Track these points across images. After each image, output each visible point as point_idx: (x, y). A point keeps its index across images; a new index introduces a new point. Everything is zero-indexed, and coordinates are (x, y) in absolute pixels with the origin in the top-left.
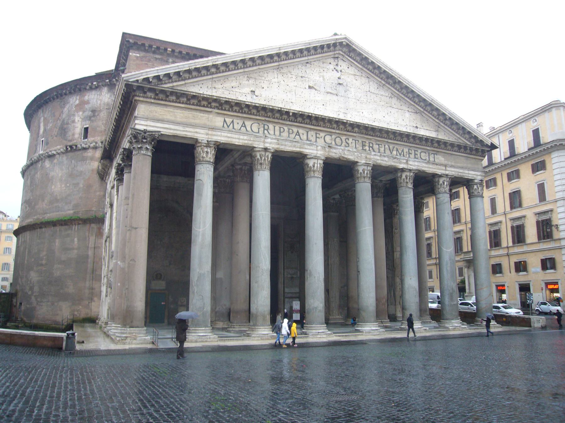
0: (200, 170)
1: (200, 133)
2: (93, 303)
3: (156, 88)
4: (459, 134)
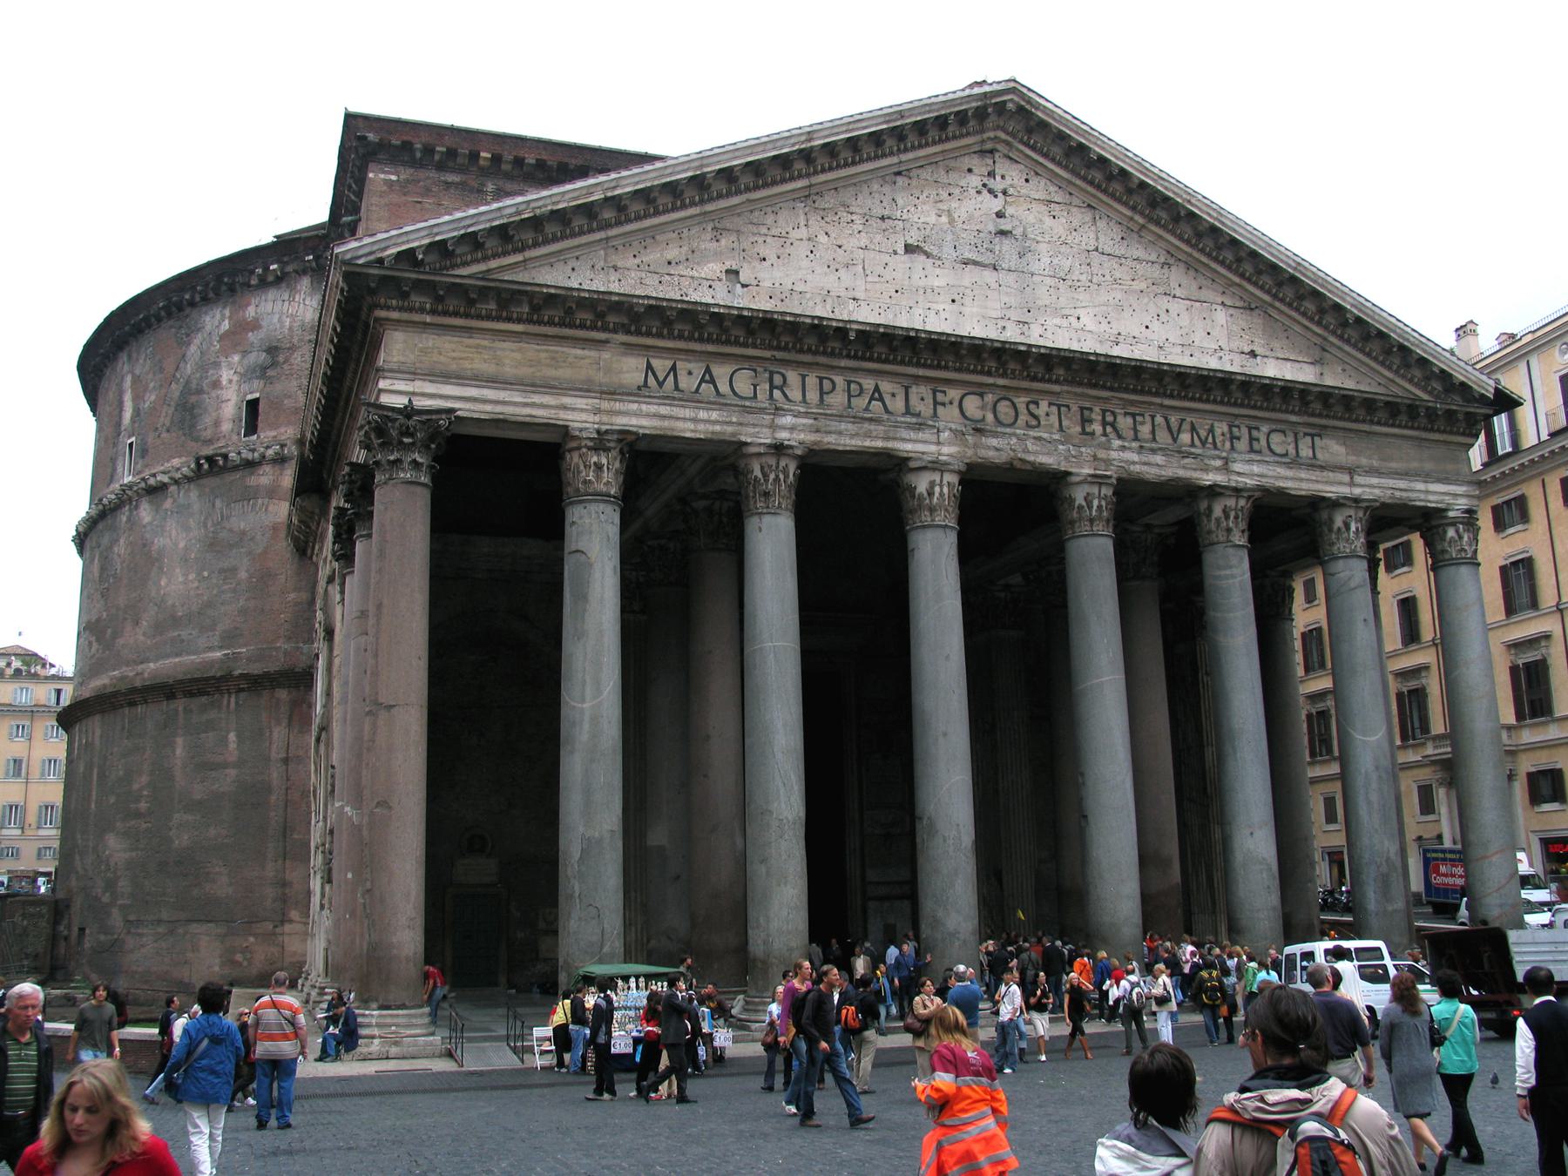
0: (579, 522)
1: (574, 409)
2: (287, 928)
3: (438, 278)
4: (1389, 368)
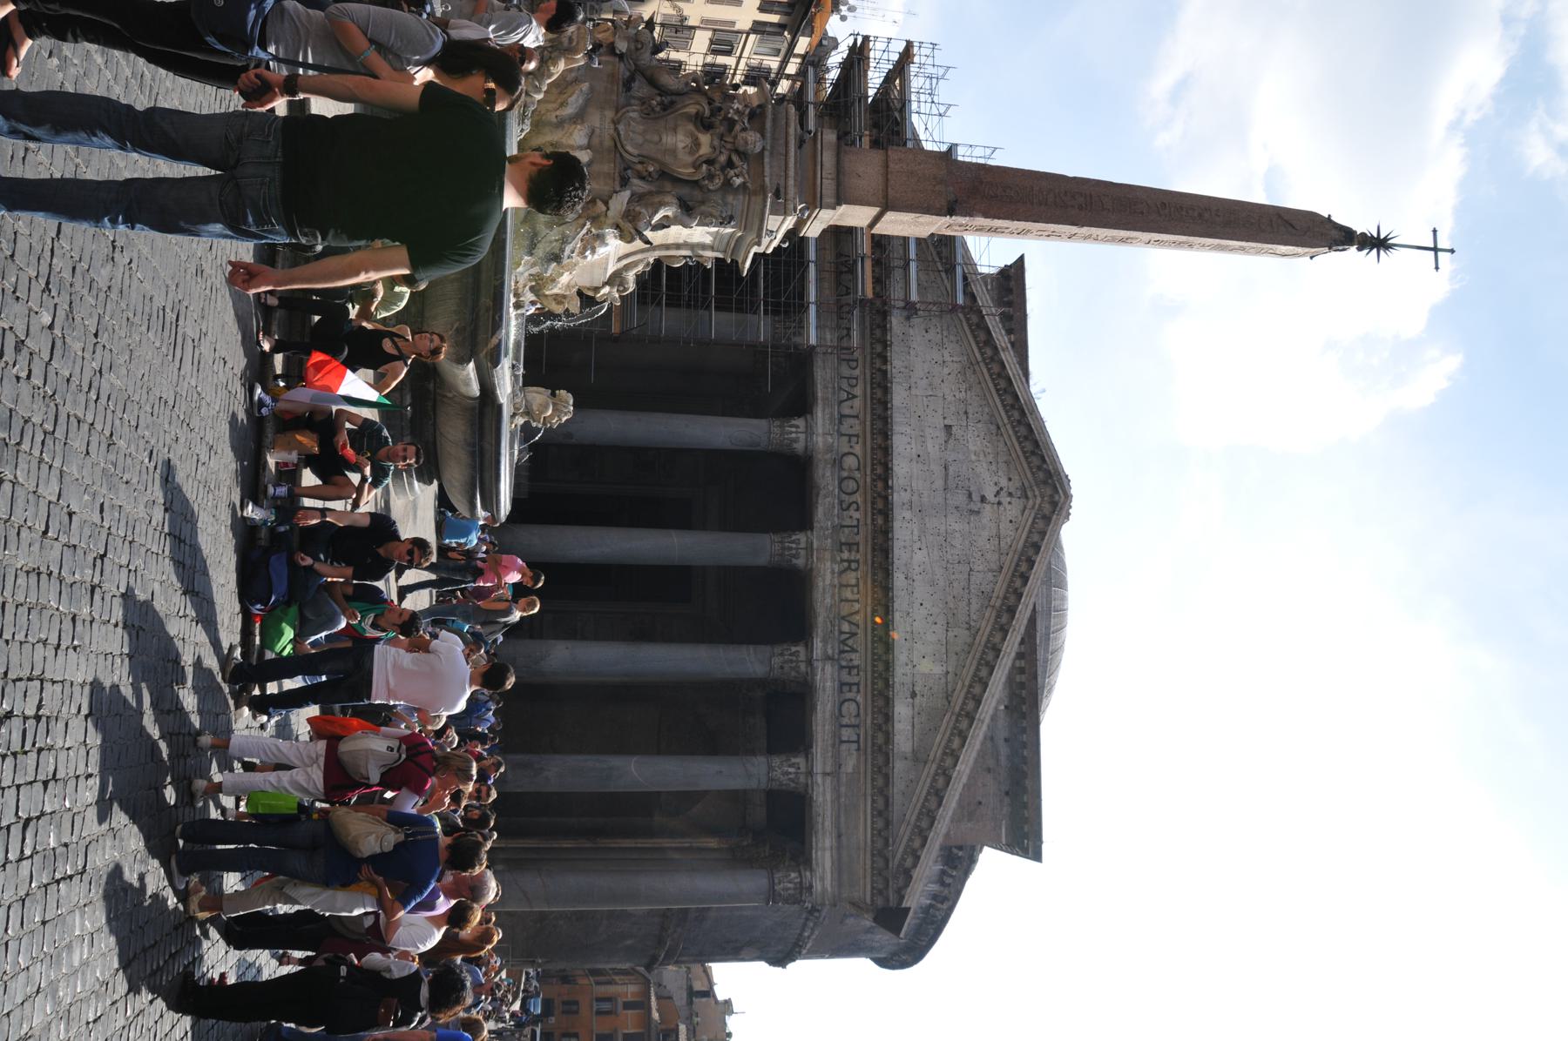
4: (918, 819)
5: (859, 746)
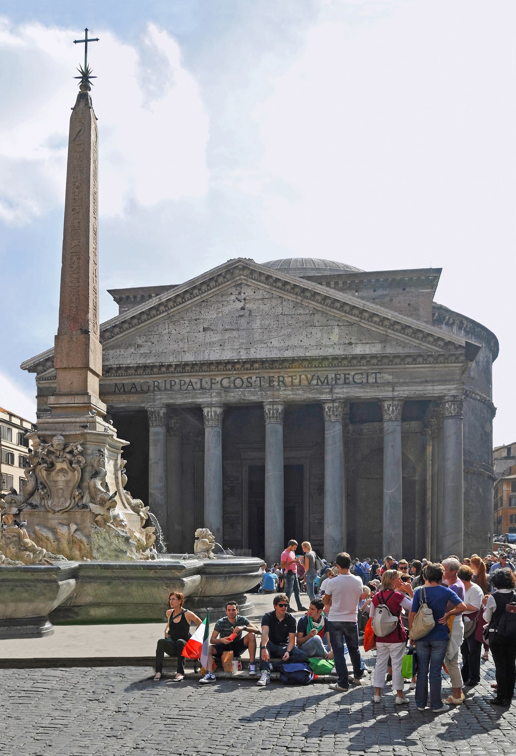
4: (418, 339)
5: (378, 373)
